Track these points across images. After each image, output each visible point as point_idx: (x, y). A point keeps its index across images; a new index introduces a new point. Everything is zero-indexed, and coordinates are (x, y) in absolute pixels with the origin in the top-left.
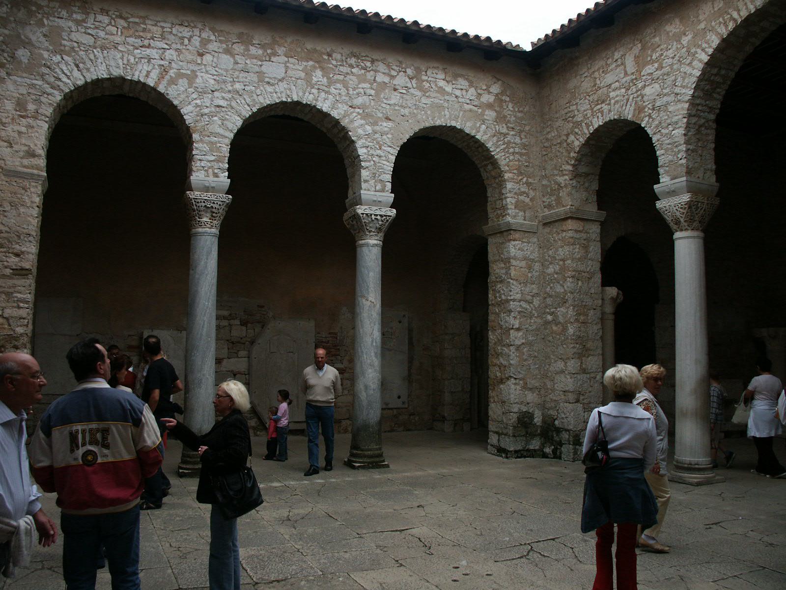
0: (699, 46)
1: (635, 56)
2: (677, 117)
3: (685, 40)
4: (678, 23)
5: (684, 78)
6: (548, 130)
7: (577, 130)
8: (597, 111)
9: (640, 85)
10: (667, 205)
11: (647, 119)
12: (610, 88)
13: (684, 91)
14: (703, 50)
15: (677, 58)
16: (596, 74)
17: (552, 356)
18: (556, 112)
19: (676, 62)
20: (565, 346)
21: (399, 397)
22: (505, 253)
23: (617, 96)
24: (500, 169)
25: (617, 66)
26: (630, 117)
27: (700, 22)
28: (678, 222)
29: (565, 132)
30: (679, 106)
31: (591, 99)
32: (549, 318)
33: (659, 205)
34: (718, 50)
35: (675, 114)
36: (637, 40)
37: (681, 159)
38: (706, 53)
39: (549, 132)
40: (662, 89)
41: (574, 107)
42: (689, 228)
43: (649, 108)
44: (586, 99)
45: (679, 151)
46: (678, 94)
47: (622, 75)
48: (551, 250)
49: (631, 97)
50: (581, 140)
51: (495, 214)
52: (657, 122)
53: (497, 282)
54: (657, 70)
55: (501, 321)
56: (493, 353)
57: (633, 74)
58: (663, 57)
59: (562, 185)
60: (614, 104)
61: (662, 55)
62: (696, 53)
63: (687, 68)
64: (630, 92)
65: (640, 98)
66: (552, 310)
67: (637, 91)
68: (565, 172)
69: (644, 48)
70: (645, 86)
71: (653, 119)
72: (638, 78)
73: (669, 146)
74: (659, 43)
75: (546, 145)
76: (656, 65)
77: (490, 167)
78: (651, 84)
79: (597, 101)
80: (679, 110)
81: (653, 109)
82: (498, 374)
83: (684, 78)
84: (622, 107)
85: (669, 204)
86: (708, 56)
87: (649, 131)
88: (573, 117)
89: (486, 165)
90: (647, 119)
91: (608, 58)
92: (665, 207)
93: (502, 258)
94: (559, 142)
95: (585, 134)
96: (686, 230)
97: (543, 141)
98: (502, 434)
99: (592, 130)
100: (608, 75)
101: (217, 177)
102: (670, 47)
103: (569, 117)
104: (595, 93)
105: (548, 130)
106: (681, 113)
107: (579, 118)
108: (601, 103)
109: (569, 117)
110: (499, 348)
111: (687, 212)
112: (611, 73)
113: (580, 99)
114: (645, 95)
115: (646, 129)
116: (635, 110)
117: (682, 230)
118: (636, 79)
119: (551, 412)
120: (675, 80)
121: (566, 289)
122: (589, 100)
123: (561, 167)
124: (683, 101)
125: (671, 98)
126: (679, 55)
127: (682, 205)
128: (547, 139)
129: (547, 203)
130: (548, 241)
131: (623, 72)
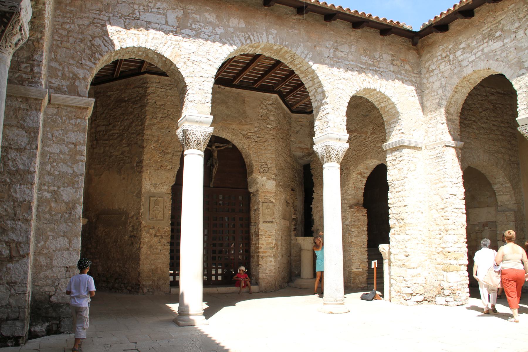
0: (228, 40)
1: (177, 16)
4: (215, 17)
6: (65, 20)
12: (149, 24)
17: (49, 233)
20: (70, 224)
22: (28, 120)
24: (42, 32)
25: (160, 14)
29: (91, 33)
32: (48, 195)
36: (180, 7)
44: (120, 18)
48: (57, 131)
51: (17, 75)
53: (11, 148)
54: (195, 36)
55: (16, 192)
57: (173, 26)
59: (81, 77)
61: (200, 29)
66: (52, 188)
68: (85, 67)
69: (185, 15)
72: (178, 32)
74: (199, 20)
75: (60, 31)
81: (188, 60)
85: (196, 129)
87: (183, 73)
91: (149, 2)
93: (21, 124)
94: (80, 37)
97: (57, 27)
98: (7, 319)
102: (207, 28)
105: (65, 20)
110: (9, 222)
112: (152, 14)
119: (47, 289)
121: (76, 170)
122: (125, 22)
123: (81, 60)
125: (205, 60)
128: (64, 29)
129: (56, 85)
130: (54, 121)
131: (164, 20)
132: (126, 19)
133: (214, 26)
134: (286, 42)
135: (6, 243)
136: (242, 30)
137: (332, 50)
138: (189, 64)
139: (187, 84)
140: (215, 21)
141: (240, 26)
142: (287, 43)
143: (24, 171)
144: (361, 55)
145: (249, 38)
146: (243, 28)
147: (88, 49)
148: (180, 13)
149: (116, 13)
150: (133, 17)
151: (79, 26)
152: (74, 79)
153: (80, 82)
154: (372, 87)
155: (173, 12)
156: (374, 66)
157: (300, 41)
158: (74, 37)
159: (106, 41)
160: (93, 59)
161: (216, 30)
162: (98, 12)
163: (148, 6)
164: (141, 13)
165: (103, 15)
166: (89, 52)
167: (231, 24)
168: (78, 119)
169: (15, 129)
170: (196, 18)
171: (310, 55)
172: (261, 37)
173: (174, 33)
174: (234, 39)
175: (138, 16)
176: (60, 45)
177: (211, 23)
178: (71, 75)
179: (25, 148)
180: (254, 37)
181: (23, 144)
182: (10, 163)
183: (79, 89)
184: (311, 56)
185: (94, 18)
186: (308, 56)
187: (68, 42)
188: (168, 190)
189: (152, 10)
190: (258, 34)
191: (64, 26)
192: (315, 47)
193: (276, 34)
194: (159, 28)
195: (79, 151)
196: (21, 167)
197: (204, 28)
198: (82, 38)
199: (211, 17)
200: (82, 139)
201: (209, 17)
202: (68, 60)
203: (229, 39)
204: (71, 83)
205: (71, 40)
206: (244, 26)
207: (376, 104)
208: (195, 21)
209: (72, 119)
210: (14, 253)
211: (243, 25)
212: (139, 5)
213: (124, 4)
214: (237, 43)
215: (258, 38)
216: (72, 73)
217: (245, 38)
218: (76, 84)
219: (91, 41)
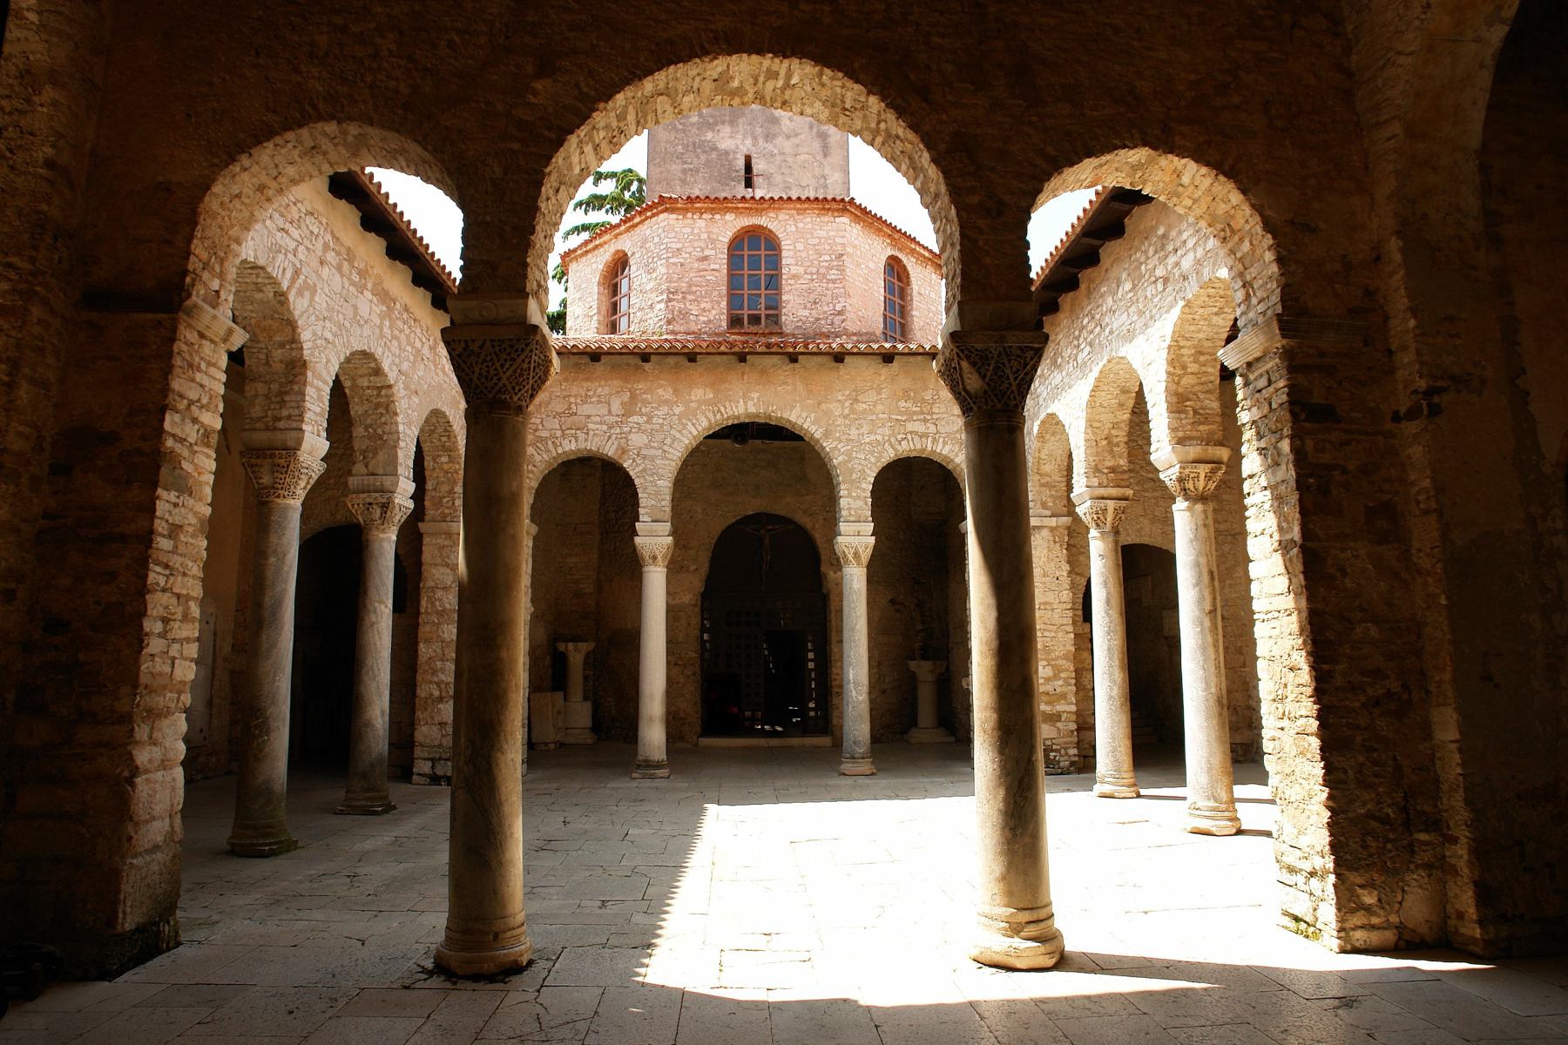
0: (689, 420)
3: (677, 410)
5: (674, 441)
7: (540, 446)
13: (671, 450)
16: (572, 400)
21: (201, 731)
23: (597, 429)
25: (601, 402)
28: (655, 558)
30: (667, 462)
34: (704, 429)
44: (555, 417)
45: (663, 500)
49: (614, 436)
50: (545, 456)
55: (443, 632)
56: (427, 668)
65: (623, 440)
69: (633, 397)
76: (645, 418)
77: (445, 459)
82: (436, 693)
87: (631, 473)
88: (535, 430)
89: (439, 456)
98: (440, 759)
99: (560, 450)
101: (319, 435)
107: (545, 434)
116: (617, 449)
125: (659, 453)
131: (606, 409)
135: (436, 683)
136: (709, 403)
137: (847, 404)
141: (707, 397)
143: (450, 610)
144: (900, 400)
145: (719, 411)
154: (918, 446)
156: (923, 413)
163: (586, 395)
167: (693, 398)
169: (441, 568)
172: (736, 407)
177: (666, 402)
179: (450, 587)
180: (726, 408)
181: (449, 583)
182: (438, 603)
188: (691, 599)
192: (819, 404)
193: (759, 398)
196: (448, 606)
197: (658, 409)
199: (665, 393)
206: (711, 396)
207: (944, 464)
208: (645, 403)
210: (444, 694)
212: (576, 396)
217: (713, 412)
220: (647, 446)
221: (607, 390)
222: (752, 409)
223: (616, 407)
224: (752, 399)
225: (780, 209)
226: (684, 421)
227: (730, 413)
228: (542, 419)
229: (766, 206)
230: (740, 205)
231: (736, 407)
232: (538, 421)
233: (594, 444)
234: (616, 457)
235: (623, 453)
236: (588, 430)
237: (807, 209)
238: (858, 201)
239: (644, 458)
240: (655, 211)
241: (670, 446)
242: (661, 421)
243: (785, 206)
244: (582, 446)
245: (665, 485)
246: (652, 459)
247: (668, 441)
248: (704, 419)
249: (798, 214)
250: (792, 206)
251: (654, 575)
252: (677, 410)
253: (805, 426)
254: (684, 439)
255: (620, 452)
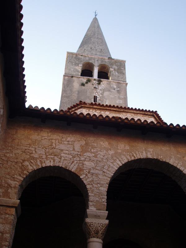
0: (117, 158)
1: (81, 145)
2: (103, 182)
3: (111, 152)
4: (107, 144)
5: (109, 167)
6: (8, 151)
7: (32, 161)
8: (50, 158)
9: (82, 159)
10: (94, 222)
11: (85, 175)
12: (62, 151)
14: (119, 160)
15: (106, 157)
18: (18, 145)
19: (105, 158)
23: (67, 157)
25: (70, 144)
26: (72, 170)
27: (118, 149)
29: (23, 158)
30: (105, 178)
31: (47, 150)
33: (88, 220)
35: (102, 180)
36: (83, 139)
37: (103, 202)
38: (121, 162)
39: (8, 153)
40: (95, 166)
41: (33, 149)
42: (101, 238)
43: (86, 171)
44: (43, 148)
45: (103, 198)
46: (105, 172)
47: (71, 149)
49: (76, 162)
50: (35, 167)
52: (90, 179)
54: (93, 157)
57: (79, 152)
58: (97, 153)
59: (13, 186)
60: (64, 160)
62: (116, 160)
63: (111, 164)
64: (75, 159)
65: (81, 164)
67: (80, 161)
68: (16, 179)
69: (87, 144)
70: (85, 160)
71: (88, 177)
73: (97, 193)
74: (96, 147)
75: (3, 158)
78: (89, 161)
79: (52, 154)
80: (105, 180)
81: (89, 173)
83: (109, 167)
84: (68, 164)
85: (95, 222)
86: (122, 164)
87: (85, 182)
88: (32, 153)
90: (85, 175)
91: (63, 138)
92: (92, 222)
95: (38, 165)
96: (100, 238)
99: (44, 165)
100: (62, 145)
102: (102, 151)
103: (28, 152)
104: (51, 149)
105: (8, 151)
106: (106, 181)
107: (36, 156)
108: (54, 156)
109: (28, 152)
111: (104, 229)
112: (64, 145)
113: (38, 147)
114: (85, 164)
115: (82, 180)
116: (77, 168)
117: (98, 238)
118: (80, 155)
120: (104, 166)
123: (14, 175)
124: (107, 177)
125: (101, 172)
126: (107, 156)
127: (103, 225)
132: (46, 149)
133: (107, 150)
134: (160, 156)
138: (89, 175)
139: (88, 189)
140: (107, 147)
142: (161, 157)
145: (133, 155)
146: (127, 149)
147: (20, 169)
148: (83, 143)
149: (40, 146)
150: (51, 147)
151: (15, 154)
152: (8, 188)
153: (11, 189)
155: (78, 143)
157: (172, 154)
158: (11, 161)
159: (32, 163)
160: (22, 175)
161: (108, 152)
162: (29, 146)
163: (61, 140)
164: (57, 145)
165: (31, 147)
166: (20, 170)
167: (119, 148)
168: (7, 215)
170: (94, 145)
171: (180, 163)
173: (79, 155)
174: (122, 157)
175: (54, 147)
176: (2, 167)
178: (6, 185)
180: (136, 155)
183: (10, 194)
184: (181, 164)
185: (26, 149)
186: (179, 164)
187: (7, 164)
189: (64, 143)
190: (139, 152)
191: (6, 154)
194: (69, 153)
195: (5, 238)
197: (100, 151)
198: (16, 161)
200: (8, 229)
201: (103, 144)
202: (6, 176)
203: (118, 157)
204: (5, 190)
205: (9, 163)
206: (128, 148)
208: (93, 147)
209: (3, 215)
211: (127, 147)
213: (46, 140)
214: (124, 160)
215: (140, 155)
216: (7, 184)
217: (130, 156)
218: (9, 191)
219: (22, 163)
220: (93, 168)
221: (73, 139)
222: (150, 156)
223: (77, 147)
224: (150, 152)
225: (127, 112)
226: (115, 158)
227: (139, 157)
228: (35, 148)
229: (122, 110)
230: (112, 109)
231: (142, 155)
232: (33, 149)
233: (64, 164)
234: (76, 173)
235: (80, 171)
236: (61, 157)
237: (138, 114)
238: (158, 113)
239: (93, 174)
240: (77, 108)
241: (107, 170)
242: (102, 157)
243: (130, 111)
244: (57, 165)
245: (104, 189)
246: (97, 175)
247: (106, 167)
248: (125, 158)
249: (135, 115)
250: (132, 111)
251: (94, 244)
252: (111, 152)
253: (178, 167)
254: (114, 167)
255: (78, 170)
